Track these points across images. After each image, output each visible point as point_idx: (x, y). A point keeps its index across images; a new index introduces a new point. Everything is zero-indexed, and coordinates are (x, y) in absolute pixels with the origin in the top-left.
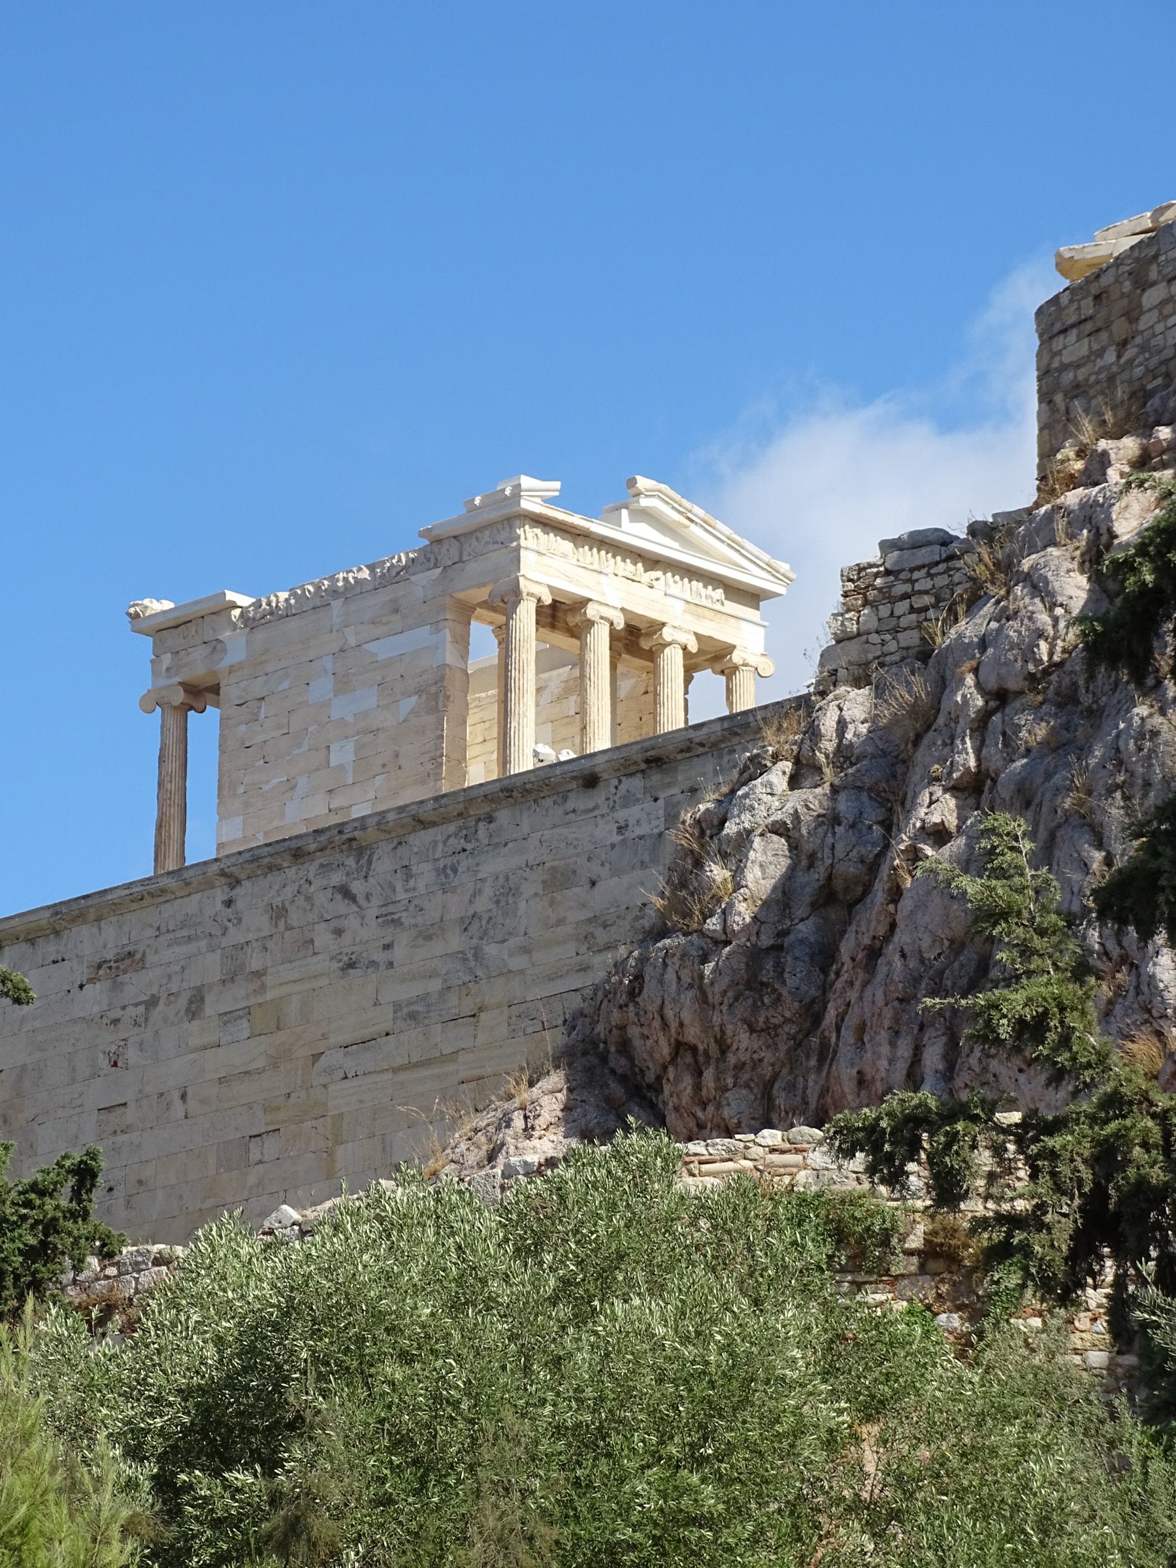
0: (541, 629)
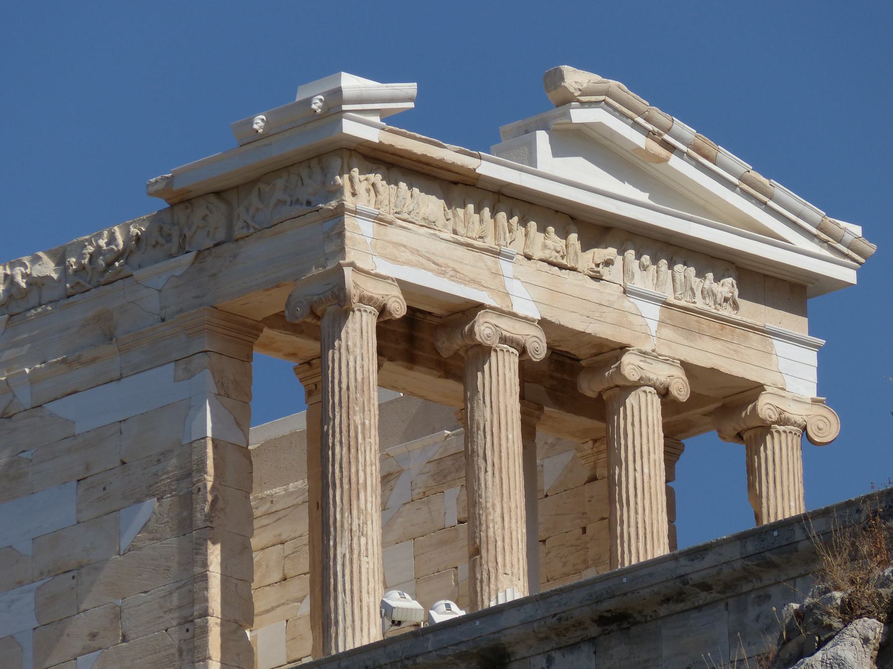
0: (387, 364)
